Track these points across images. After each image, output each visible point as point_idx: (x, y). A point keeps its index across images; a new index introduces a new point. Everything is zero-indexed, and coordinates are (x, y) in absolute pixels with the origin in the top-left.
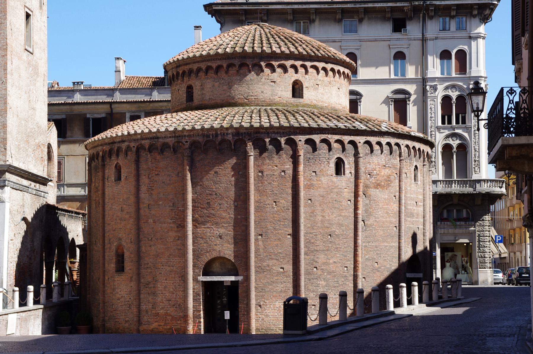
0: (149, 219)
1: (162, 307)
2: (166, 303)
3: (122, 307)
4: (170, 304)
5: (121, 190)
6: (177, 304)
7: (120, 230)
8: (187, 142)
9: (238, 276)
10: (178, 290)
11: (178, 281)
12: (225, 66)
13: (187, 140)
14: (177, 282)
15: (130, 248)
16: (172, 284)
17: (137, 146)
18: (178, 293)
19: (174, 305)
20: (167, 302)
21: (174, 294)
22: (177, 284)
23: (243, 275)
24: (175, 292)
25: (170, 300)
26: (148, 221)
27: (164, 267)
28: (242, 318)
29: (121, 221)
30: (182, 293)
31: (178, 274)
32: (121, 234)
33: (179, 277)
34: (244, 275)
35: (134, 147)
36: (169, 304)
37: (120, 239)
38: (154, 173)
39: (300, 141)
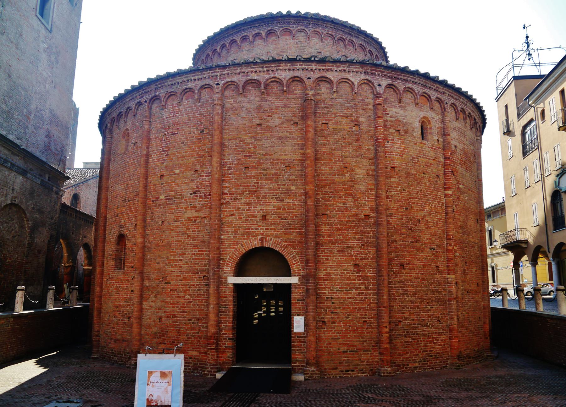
0: (161, 195)
1: (172, 322)
2: (179, 316)
3: (119, 320)
4: (185, 317)
5: (127, 162)
6: (196, 318)
7: (123, 215)
8: (218, 84)
9: (291, 276)
10: (198, 297)
11: (198, 284)
12: (263, 33)
13: (219, 81)
14: (197, 285)
15: (133, 237)
16: (190, 287)
17: (150, 100)
18: (197, 301)
19: (190, 320)
20: (180, 315)
21: (191, 302)
22: (196, 288)
23: (298, 275)
24: (193, 300)
25: (186, 312)
26: (159, 198)
27: (177, 262)
28: (296, 342)
29: (124, 202)
30: (203, 301)
31: (198, 273)
32: (123, 219)
33: (200, 278)
34: (300, 275)
35: (146, 101)
36: (183, 317)
37: (122, 226)
38: (170, 132)
39: (379, 85)
